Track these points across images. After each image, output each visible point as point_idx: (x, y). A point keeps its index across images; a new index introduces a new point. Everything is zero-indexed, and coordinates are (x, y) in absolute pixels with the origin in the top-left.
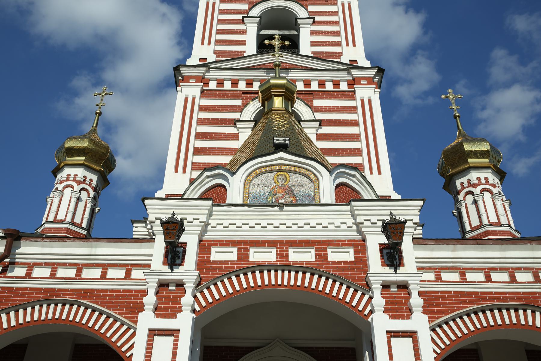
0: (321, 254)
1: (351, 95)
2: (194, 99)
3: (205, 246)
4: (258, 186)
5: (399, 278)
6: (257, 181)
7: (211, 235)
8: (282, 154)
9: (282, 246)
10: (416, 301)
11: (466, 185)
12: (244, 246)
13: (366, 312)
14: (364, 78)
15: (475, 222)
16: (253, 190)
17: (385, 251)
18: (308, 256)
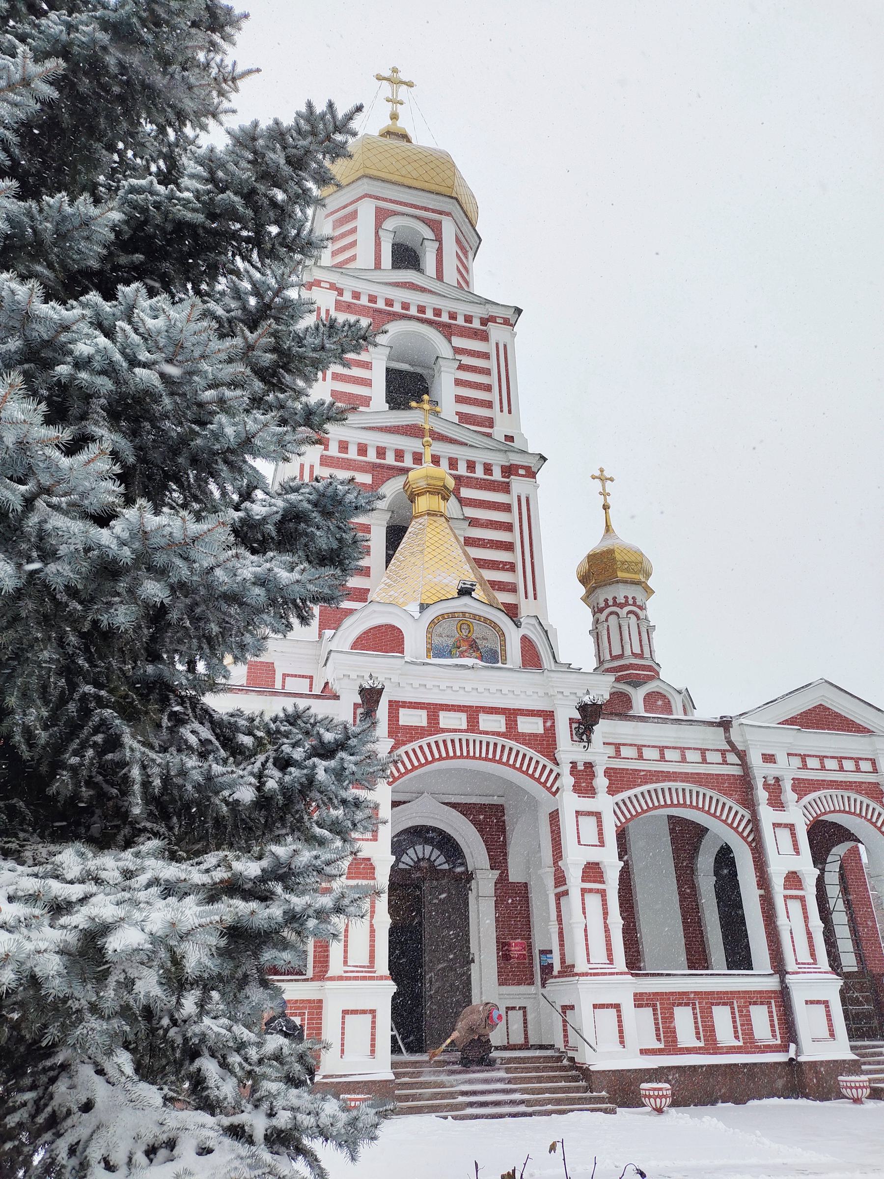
0: (512, 724)
1: (505, 488)
2: (312, 467)
4: (440, 636)
5: (588, 758)
6: (439, 630)
8: (466, 600)
9: (473, 713)
10: (601, 782)
11: (611, 603)
12: (433, 710)
13: (554, 789)
14: (523, 467)
15: (617, 651)
16: (436, 640)
17: (574, 725)
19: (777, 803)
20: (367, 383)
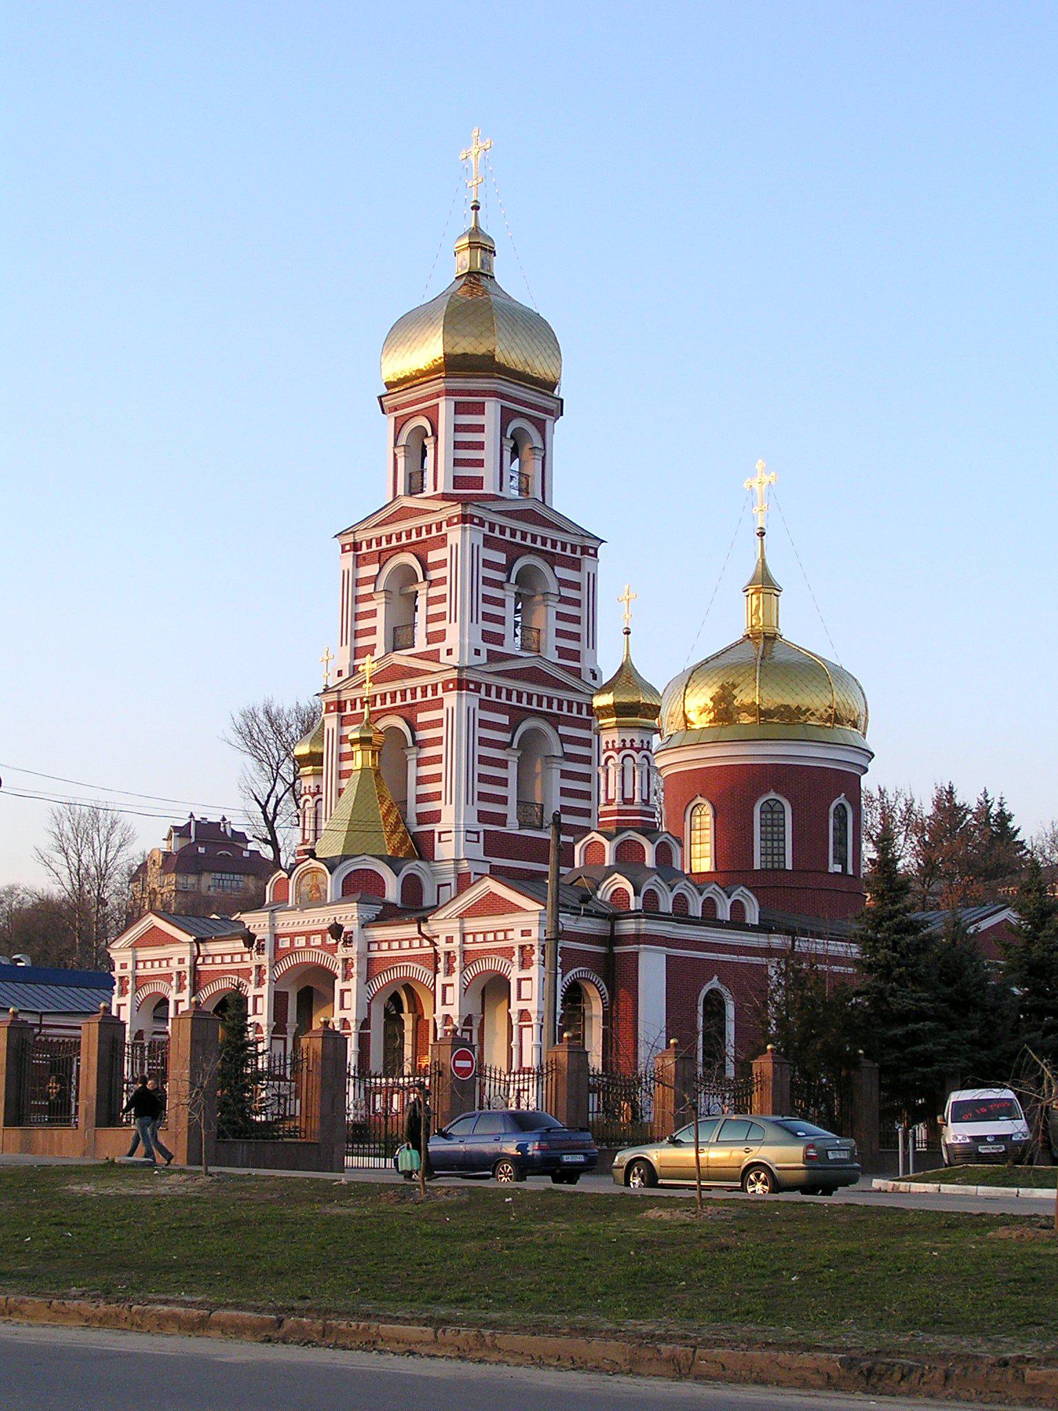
1: (439, 704)
3: (277, 937)
6: (304, 882)
7: (279, 931)
9: (308, 935)
12: (292, 936)
18: (317, 940)
19: (449, 971)
20: (372, 631)
